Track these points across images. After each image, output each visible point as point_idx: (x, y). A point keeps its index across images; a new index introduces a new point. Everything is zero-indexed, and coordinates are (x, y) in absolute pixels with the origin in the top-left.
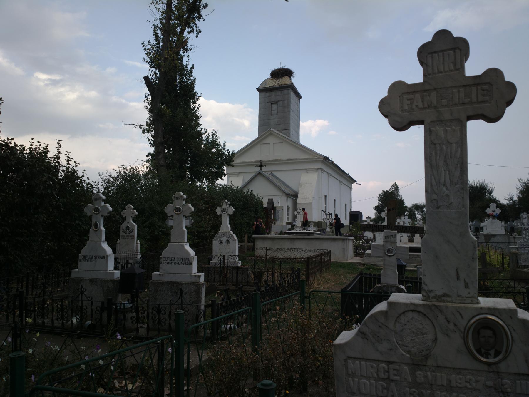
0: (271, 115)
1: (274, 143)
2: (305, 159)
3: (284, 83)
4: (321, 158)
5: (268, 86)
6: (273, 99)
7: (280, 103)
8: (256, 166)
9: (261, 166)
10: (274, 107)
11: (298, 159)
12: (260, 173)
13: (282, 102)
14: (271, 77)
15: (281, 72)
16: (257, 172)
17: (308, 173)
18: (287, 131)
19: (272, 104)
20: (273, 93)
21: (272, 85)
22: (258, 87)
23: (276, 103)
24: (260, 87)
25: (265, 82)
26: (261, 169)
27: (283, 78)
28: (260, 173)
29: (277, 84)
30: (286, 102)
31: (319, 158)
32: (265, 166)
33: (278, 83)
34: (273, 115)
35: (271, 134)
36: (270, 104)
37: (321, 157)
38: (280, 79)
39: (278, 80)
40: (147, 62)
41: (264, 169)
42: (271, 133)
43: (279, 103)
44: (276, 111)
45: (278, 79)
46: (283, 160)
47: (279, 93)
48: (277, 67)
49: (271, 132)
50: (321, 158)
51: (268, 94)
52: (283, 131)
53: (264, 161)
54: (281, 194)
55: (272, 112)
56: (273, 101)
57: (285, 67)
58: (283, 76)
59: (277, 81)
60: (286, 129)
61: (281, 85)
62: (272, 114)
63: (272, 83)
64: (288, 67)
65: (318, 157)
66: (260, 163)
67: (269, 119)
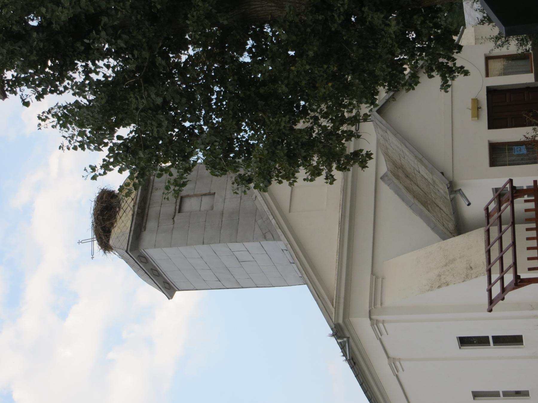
51: (151, 225)
56: (174, 208)
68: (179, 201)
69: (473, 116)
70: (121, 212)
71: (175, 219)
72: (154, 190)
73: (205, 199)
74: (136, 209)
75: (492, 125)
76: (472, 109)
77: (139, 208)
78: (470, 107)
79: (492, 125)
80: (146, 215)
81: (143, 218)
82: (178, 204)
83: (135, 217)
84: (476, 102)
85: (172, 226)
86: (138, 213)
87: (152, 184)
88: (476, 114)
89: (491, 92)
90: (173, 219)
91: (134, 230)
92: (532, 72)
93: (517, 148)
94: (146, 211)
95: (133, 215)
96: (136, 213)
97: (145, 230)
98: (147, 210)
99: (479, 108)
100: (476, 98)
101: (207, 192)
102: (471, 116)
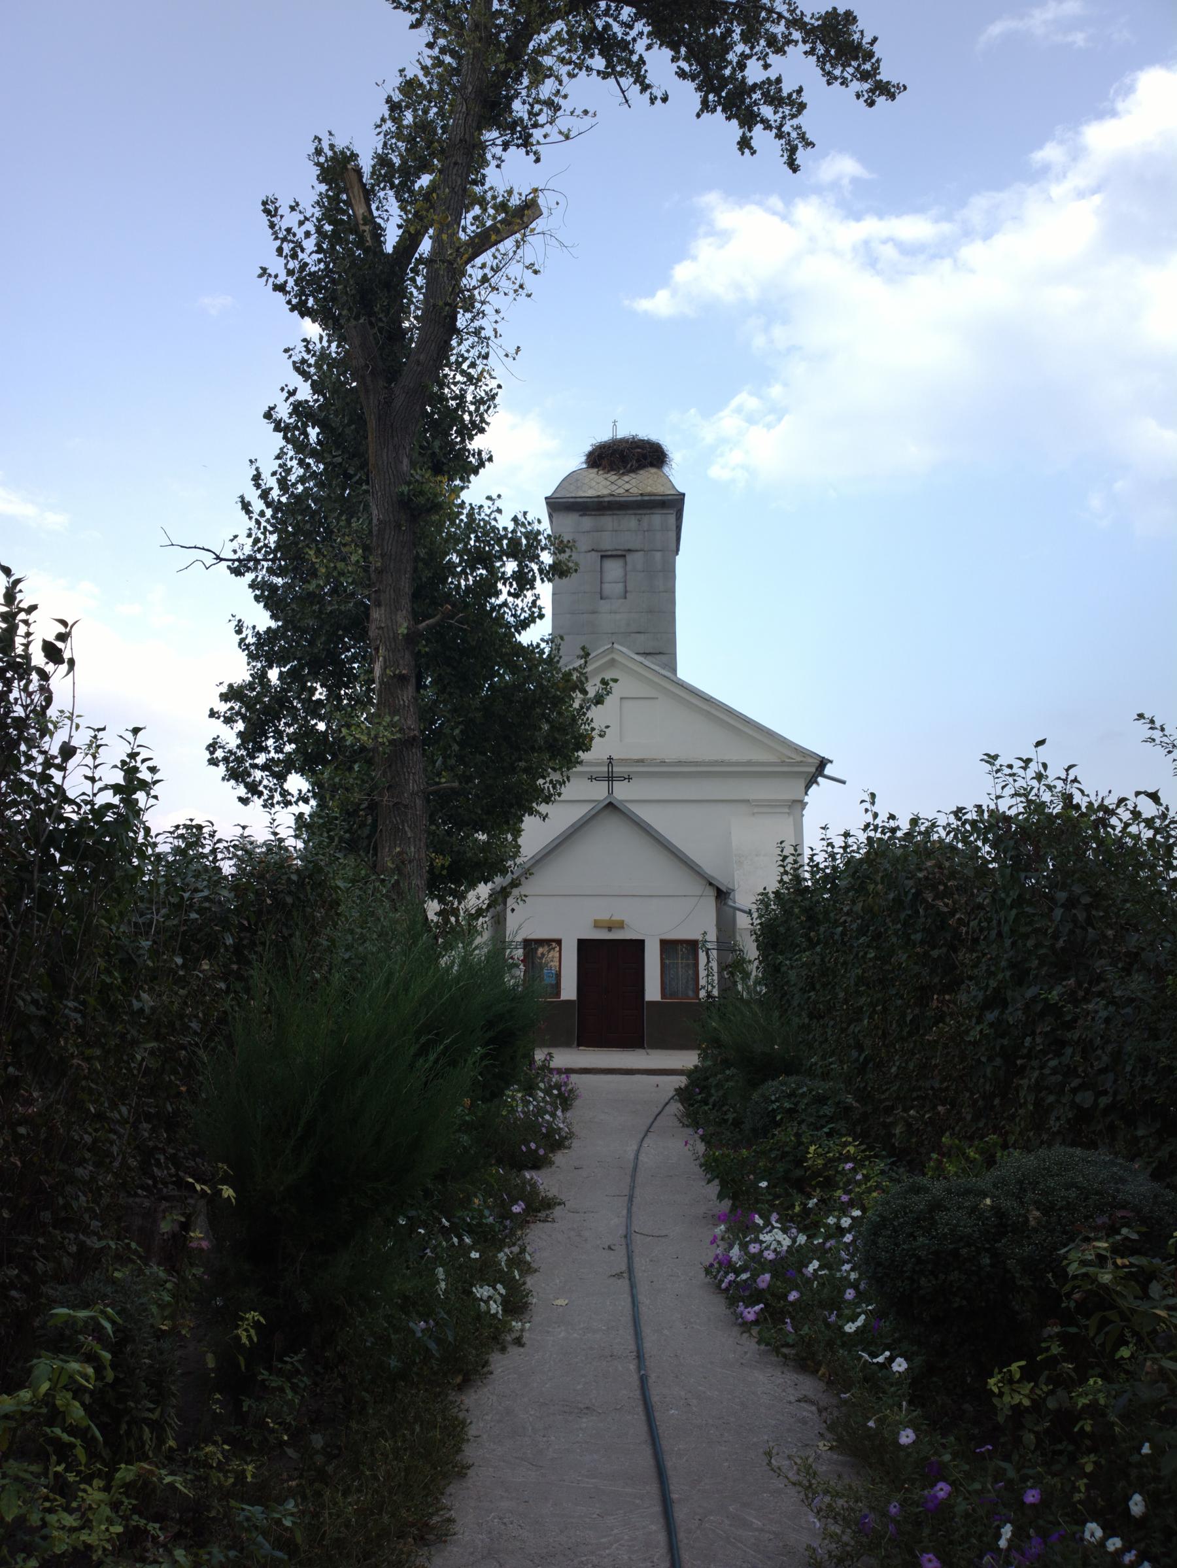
0: (601, 598)
1: (621, 698)
2: (749, 763)
3: (649, 489)
4: (809, 765)
6: (608, 542)
7: (635, 559)
8: (591, 779)
9: (610, 778)
10: (613, 569)
11: (722, 763)
12: (610, 804)
14: (584, 466)
16: (599, 801)
17: (754, 814)
18: (663, 658)
19: (602, 557)
20: (608, 521)
21: (606, 492)
22: (549, 494)
23: (621, 555)
25: (571, 479)
26: (611, 792)
27: (641, 472)
28: (610, 804)
29: (621, 491)
30: (658, 555)
31: (800, 763)
32: (630, 779)
33: (627, 486)
36: (595, 556)
37: (811, 760)
38: (633, 475)
39: (626, 478)
40: (280, 288)
41: (622, 792)
43: (629, 558)
44: (621, 586)
45: (623, 474)
46: (663, 763)
47: (630, 522)
48: (604, 436)
50: (809, 765)
52: (649, 657)
53: (625, 762)
54: (697, 888)
55: (606, 586)
56: (609, 548)
59: (620, 482)
60: (660, 653)
61: (642, 495)
63: (602, 485)
65: (799, 759)
66: (606, 769)
67: (594, 612)
68: (619, 553)
69: (596, 921)
70: (614, 478)
72: (638, 517)
74: (606, 499)
75: (583, 945)
76: (610, 921)
77: (609, 502)
78: (613, 918)
79: (583, 945)
81: (598, 510)
82: (614, 553)
83: (596, 500)
84: (621, 925)
87: (648, 512)
88: (597, 925)
89: (639, 945)
95: (598, 497)
96: (601, 499)
97: (581, 515)
99: (610, 929)
101: (628, 589)
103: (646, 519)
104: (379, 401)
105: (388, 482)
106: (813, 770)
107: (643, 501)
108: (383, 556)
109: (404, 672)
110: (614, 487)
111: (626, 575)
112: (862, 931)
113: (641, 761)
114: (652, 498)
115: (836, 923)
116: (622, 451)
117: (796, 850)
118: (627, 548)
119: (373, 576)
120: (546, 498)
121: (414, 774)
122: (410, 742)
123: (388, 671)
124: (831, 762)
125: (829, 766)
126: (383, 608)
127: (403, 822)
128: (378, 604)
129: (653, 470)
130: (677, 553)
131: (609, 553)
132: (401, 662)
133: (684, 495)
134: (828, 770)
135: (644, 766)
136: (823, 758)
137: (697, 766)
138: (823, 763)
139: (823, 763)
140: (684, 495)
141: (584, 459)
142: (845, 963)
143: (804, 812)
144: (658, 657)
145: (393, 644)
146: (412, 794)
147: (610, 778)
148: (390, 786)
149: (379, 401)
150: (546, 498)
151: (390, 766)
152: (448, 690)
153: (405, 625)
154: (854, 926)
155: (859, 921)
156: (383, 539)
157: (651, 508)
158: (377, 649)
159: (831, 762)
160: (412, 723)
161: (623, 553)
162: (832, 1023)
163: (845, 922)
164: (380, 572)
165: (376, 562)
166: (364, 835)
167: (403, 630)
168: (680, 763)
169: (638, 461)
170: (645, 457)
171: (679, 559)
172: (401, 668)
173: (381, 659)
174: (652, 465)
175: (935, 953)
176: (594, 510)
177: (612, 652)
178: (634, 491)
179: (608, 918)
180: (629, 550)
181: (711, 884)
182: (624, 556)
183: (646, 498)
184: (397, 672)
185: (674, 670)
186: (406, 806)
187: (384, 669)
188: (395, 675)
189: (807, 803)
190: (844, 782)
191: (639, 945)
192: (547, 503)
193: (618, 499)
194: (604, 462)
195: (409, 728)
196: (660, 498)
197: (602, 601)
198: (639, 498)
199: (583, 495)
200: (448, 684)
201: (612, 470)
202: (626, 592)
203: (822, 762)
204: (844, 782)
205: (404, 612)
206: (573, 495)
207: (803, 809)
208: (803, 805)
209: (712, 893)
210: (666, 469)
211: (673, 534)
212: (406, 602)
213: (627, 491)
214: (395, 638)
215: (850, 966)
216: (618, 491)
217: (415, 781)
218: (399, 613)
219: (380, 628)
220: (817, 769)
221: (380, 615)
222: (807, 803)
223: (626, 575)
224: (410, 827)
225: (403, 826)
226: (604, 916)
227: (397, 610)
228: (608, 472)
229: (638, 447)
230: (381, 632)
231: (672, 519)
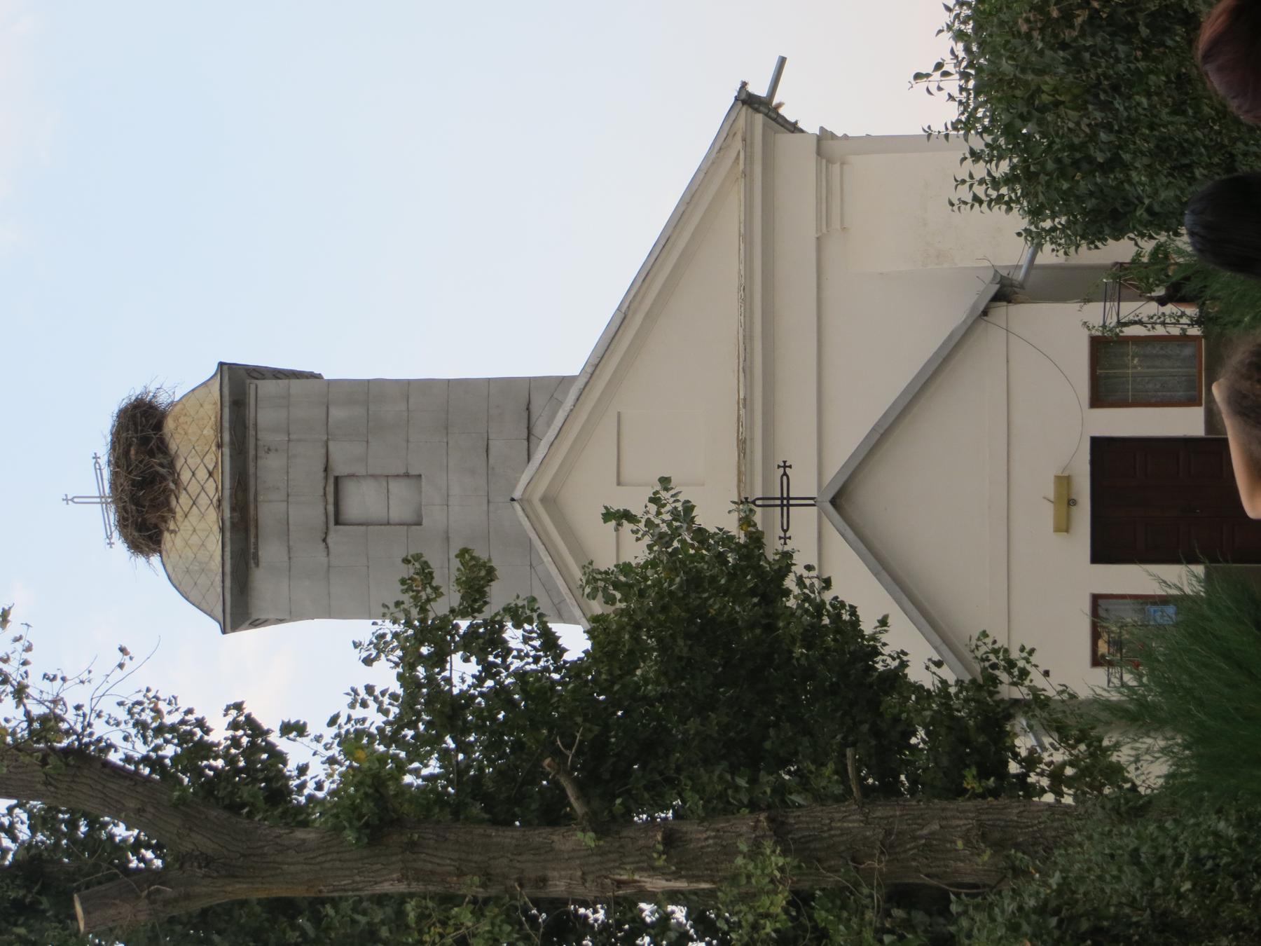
0: (419, 524)
1: (619, 484)
2: (746, 237)
3: (209, 432)
4: (750, 125)
5: (214, 545)
6: (310, 511)
11: (746, 290)
12: (834, 502)
13: (331, 444)
14: (155, 559)
15: (133, 452)
18: (538, 402)
19: (337, 523)
20: (269, 511)
21: (212, 515)
22: (216, 627)
23: (336, 484)
24: (220, 616)
25: (184, 585)
27: (173, 447)
28: (834, 502)
29: (211, 486)
30: (337, 413)
32: (785, 466)
33: (202, 474)
34: (420, 516)
35: (549, 501)
36: (337, 536)
37: (741, 123)
38: (179, 464)
39: (185, 476)
42: (544, 500)
43: (340, 469)
45: (177, 482)
46: (745, 402)
47: (270, 469)
49: (536, 499)
50: (750, 125)
51: (270, 551)
52: (537, 430)
54: (992, 338)
55: (395, 515)
56: (321, 509)
57: (104, 460)
58: (163, 447)
59: (193, 488)
60: (528, 409)
61: (220, 446)
62: (408, 515)
64: (101, 441)
65: (738, 144)
68: (331, 489)
70: (184, 499)
71: (329, 540)
72: (261, 453)
73: (399, 489)
74: (227, 514)
75: (1103, 552)
77: (233, 509)
78: (1052, 497)
79: (1103, 552)
80: (252, 523)
81: (247, 530)
82: (331, 499)
83: (228, 535)
84: (1064, 482)
85: (324, 559)
86: (233, 525)
87: (252, 432)
88: (1064, 526)
89: (1100, 447)
90: (324, 540)
91: (232, 573)
92: (1200, 405)
93: (1155, 611)
94: (252, 512)
95: (222, 530)
96: (228, 524)
97: (257, 565)
98: (252, 507)
99: (1071, 502)
100: (1066, 474)
101: (402, 471)
102: (1052, 530)
103: (266, 438)
104: (205, 876)
105: (338, 864)
106: (759, 118)
107: (232, 443)
108: (461, 874)
109: (659, 838)
110: (203, 501)
111: (373, 476)
112: (1106, 106)
113: (743, 446)
114: (226, 425)
115: (1093, 137)
116: (134, 483)
117: (963, 182)
118: (321, 474)
119: (492, 891)
120: (224, 632)
121: (832, 820)
122: (780, 831)
123: (660, 863)
124: (744, 85)
125: (752, 89)
126: (550, 874)
127: (914, 838)
128: (543, 880)
129: (169, 424)
130: (319, 377)
131: (331, 508)
132: (641, 842)
133: (221, 364)
134: (759, 89)
135: (752, 439)
136: (737, 99)
137: (752, 338)
138: (746, 100)
139: (746, 100)
140: (221, 364)
141: (141, 560)
142: (1152, 127)
143: (839, 134)
144: (535, 410)
145: (611, 856)
146: (867, 823)
147: (786, 502)
148: (854, 860)
149: (205, 876)
150: (224, 632)
151: (819, 860)
152: (672, 773)
153: (580, 835)
154: (1099, 115)
155: (1090, 107)
156: (433, 873)
157: (245, 427)
158: (620, 884)
159: (744, 85)
160: (744, 826)
161: (331, 481)
162: (1240, 145)
163: (1089, 125)
164: (488, 878)
165: (471, 887)
166: (927, 920)
167: (589, 839)
168: (746, 370)
169: (152, 454)
170: (145, 441)
171: (327, 376)
172: (651, 843)
173: (637, 877)
174: (159, 426)
175: (1144, 31)
176: (247, 539)
177: (529, 501)
178: (210, 460)
179: (1052, 505)
180: (326, 470)
181: (985, 313)
182: (337, 479)
183: (227, 437)
184: (660, 847)
185: (563, 382)
186: (888, 833)
187: (653, 870)
188: (664, 853)
189: (822, 129)
190: (782, 61)
191: (1100, 447)
192: (235, 628)
193: (227, 493)
194: (152, 518)
195: (755, 828)
196: (226, 410)
197: (424, 522)
198: (227, 450)
199: (218, 558)
200: (661, 773)
201: (167, 503)
202: (407, 475)
203: (744, 102)
204: (782, 61)
205: (555, 838)
206: (218, 578)
207: (833, 136)
208: (824, 137)
209: (1002, 311)
210: (163, 400)
211: (295, 383)
212: (540, 836)
213: (211, 474)
214: (601, 852)
215: (1157, 121)
216: (212, 492)
217: (843, 819)
218: (557, 846)
219: (584, 879)
220: (757, 111)
221: (561, 878)
222: (822, 129)
223: (373, 476)
224: (922, 827)
225: (921, 837)
226: (1048, 513)
227: (552, 850)
228: (172, 511)
229: (126, 453)
230: (590, 878)
231: (268, 387)
